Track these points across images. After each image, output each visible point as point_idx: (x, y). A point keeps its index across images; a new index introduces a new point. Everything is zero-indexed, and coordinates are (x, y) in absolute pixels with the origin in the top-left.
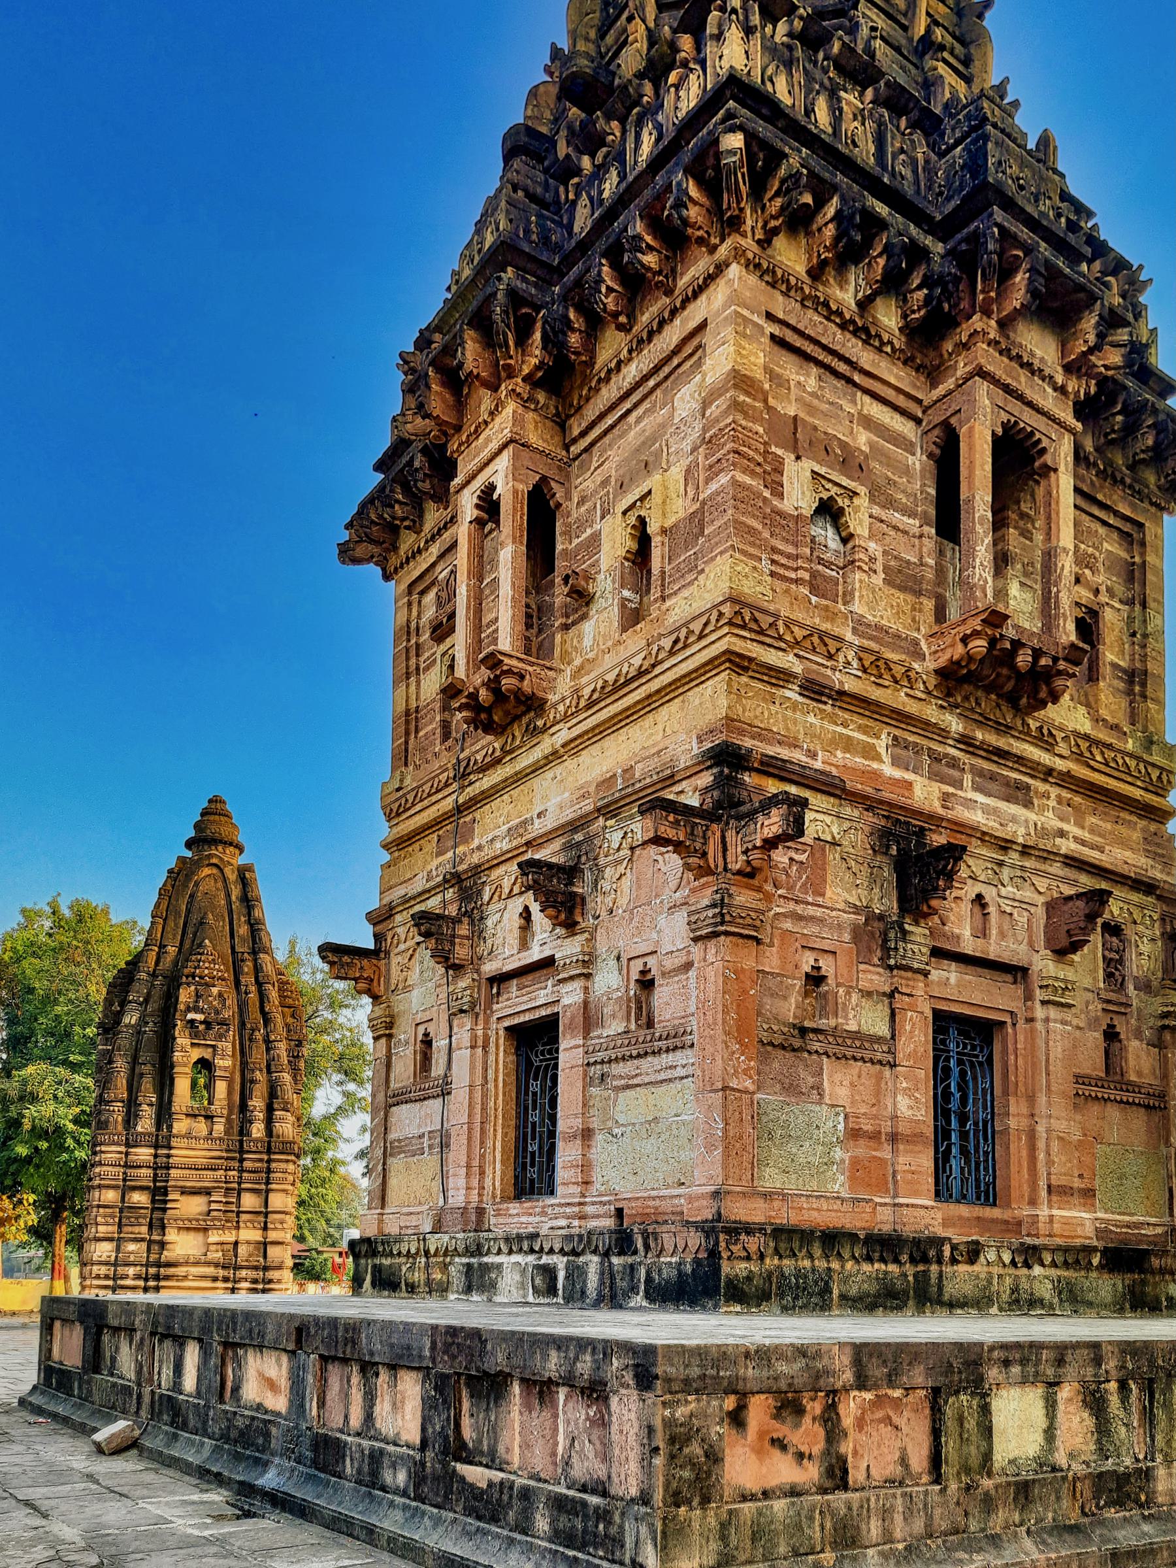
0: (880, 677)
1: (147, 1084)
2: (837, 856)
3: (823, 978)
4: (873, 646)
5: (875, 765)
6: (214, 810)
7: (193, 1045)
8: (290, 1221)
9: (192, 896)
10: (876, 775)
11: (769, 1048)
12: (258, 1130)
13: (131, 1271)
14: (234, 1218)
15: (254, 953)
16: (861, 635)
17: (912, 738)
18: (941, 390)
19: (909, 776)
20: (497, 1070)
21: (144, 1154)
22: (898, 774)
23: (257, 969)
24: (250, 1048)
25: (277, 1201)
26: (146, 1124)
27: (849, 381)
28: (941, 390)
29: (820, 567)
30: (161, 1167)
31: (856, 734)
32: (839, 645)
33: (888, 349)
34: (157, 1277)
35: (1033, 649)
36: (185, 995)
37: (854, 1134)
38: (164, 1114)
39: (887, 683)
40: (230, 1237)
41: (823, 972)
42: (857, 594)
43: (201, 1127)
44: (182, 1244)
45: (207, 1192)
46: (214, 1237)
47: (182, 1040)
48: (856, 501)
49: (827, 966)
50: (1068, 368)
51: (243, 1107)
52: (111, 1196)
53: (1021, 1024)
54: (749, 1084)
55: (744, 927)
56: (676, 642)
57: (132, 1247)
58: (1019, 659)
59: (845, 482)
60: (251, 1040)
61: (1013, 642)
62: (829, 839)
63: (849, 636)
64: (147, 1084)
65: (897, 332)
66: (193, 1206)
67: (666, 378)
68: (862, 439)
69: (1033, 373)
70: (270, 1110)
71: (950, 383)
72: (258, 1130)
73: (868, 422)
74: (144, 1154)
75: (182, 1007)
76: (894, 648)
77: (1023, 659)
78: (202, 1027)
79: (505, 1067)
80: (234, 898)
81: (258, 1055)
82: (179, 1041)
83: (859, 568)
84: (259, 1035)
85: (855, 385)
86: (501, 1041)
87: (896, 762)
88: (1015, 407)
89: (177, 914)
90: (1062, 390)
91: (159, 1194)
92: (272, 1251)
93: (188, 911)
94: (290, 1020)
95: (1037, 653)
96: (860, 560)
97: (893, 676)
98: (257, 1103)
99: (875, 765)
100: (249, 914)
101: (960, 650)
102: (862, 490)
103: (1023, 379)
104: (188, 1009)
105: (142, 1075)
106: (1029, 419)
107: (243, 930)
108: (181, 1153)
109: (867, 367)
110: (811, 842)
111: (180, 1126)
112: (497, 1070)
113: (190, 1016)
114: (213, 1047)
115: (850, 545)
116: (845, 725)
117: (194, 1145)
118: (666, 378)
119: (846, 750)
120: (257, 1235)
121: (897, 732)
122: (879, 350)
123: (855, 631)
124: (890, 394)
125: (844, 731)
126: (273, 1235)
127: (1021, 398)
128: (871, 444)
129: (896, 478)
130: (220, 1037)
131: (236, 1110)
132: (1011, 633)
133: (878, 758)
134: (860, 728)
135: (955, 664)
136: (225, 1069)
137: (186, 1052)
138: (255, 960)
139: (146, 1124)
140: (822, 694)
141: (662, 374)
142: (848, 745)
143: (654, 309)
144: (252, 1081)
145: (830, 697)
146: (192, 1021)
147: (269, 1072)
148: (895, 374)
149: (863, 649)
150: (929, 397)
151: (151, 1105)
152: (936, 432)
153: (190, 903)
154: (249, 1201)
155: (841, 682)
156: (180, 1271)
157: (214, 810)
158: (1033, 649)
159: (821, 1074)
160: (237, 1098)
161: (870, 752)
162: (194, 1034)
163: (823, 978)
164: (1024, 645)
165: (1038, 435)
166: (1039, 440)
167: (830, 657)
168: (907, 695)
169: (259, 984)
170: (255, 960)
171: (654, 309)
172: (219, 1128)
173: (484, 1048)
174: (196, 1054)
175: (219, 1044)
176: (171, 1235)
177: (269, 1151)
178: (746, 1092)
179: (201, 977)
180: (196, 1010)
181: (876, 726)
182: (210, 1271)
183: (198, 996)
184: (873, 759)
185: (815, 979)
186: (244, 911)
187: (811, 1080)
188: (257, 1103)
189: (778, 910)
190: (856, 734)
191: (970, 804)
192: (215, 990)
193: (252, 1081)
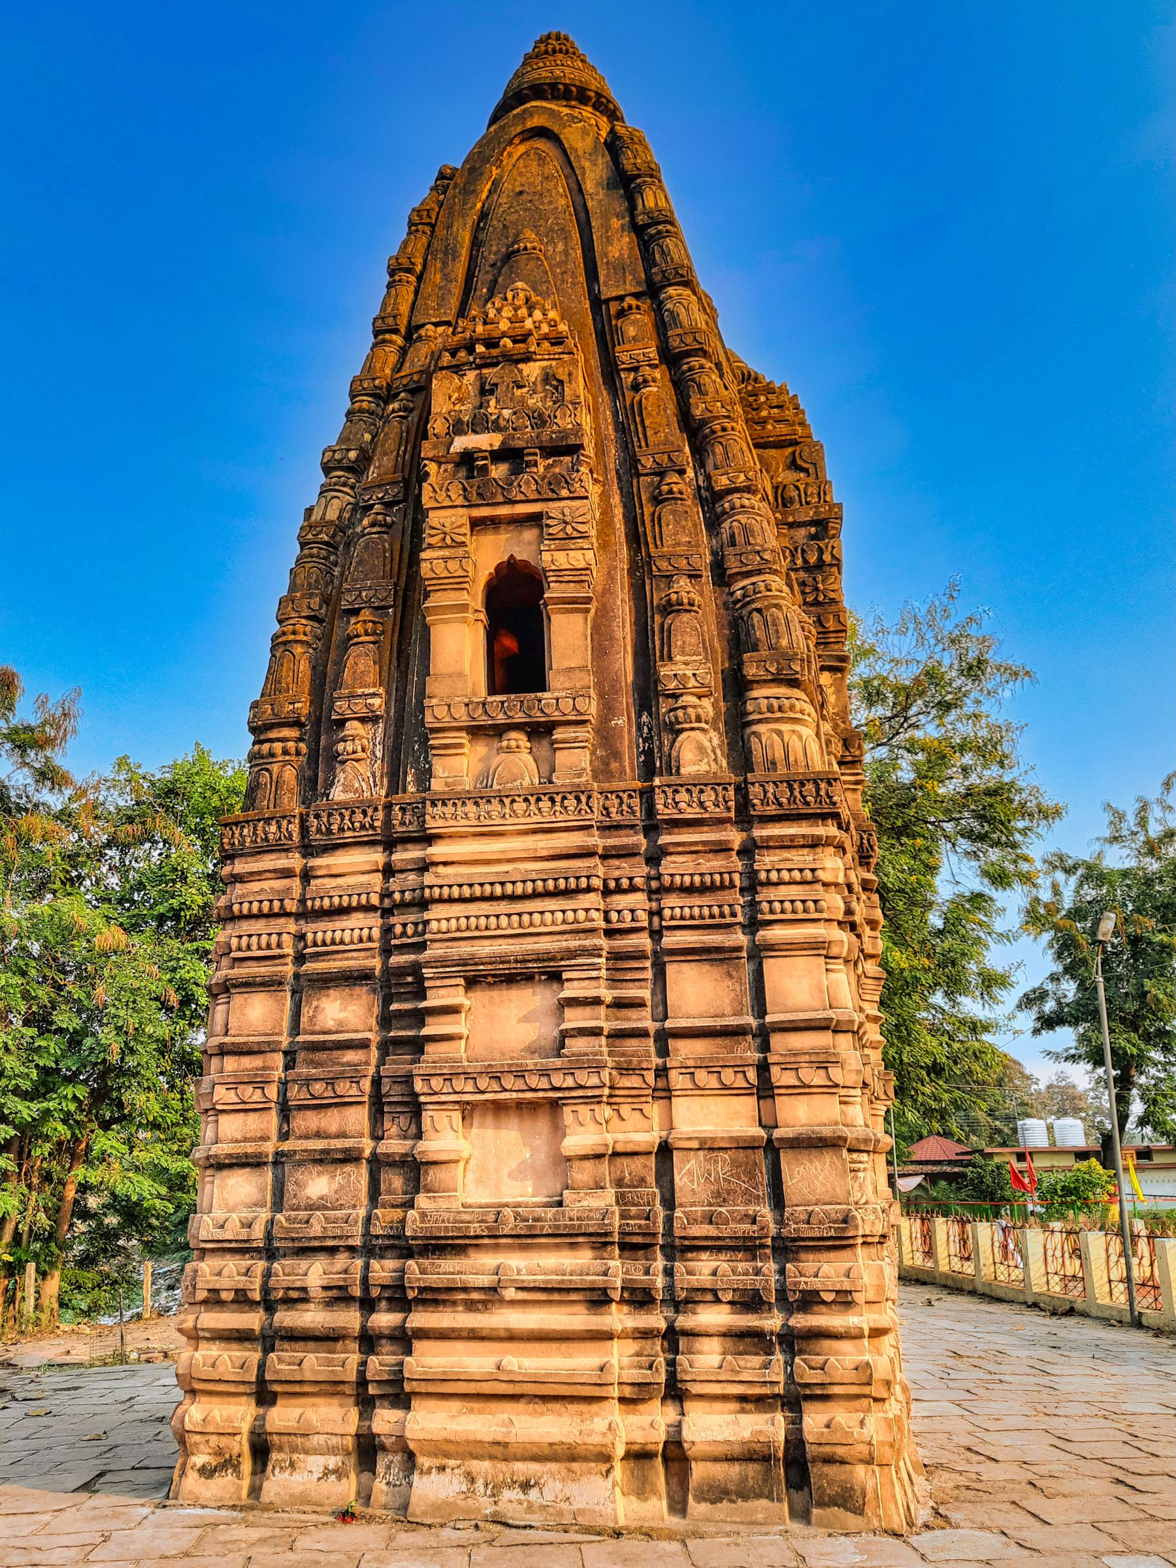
7: (477, 524)
8: (859, 1061)
9: (484, 215)
12: (699, 752)
13: (315, 1274)
14: (651, 1055)
15: (652, 291)
21: (353, 869)
24: (657, 520)
25: (795, 985)
30: (403, 905)
34: (399, 1296)
38: (410, 742)
40: (639, 1130)
43: (520, 762)
44: (482, 1167)
46: (583, 1133)
47: (446, 515)
51: (648, 690)
57: (318, 1185)
60: (657, 500)
66: (500, 1027)
70: (736, 686)
72: (699, 752)
74: (353, 869)
75: (438, 426)
78: (498, 471)
80: (589, 186)
81: (682, 535)
82: (434, 518)
84: (685, 483)
89: (450, 252)
91: (401, 992)
92: (806, 1178)
93: (476, 244)
94: (787, 477)
98: (691, 666)
100: (632, 208)
104: (458, 428)
105: (348, 641)
107: (618, 246)
111: (459, 765)
113: (461, 443)
114: (535, 519)
120: (734, 1118)
126: (799, 1115)
130: (553, 488)
131: (626, 700)
136: (580, 575)
137: (465, 559)
138: (658, 309)
139: (358, 778)
144: (669, 608)
146: (467, 458)
147: (721, 576)
151: (369, 719)
153: (477, 230)
154: (697, 993)
156: (477, 1269)
160: (624, 663)
170: (658, 309)
172: (575, 761)
174: (488, 554)
175: (553, 508)
176: (445, 1137)
177: (745, 817)
179: (491, 343)
180: (479, 424)
182: (575, 1263)
183: (486, 390)
186: (621, 206)
188: (691, 666)
192: (532, 371)
193: (669, 608)
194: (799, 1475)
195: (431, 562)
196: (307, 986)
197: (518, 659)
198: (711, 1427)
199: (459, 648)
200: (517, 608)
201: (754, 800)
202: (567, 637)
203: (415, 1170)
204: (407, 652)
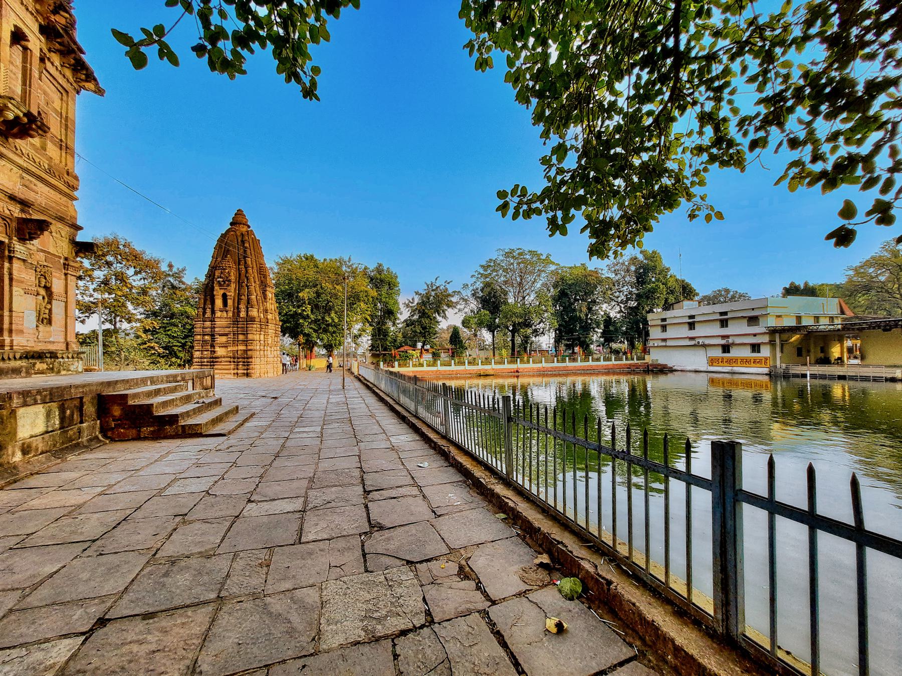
1: (208, 302)
6: (239, 213)
14: (236, 342)
15: (245, 257)
21: (208, 324)
23: (245, 263)
26: (208, 314)
30: (213, 328)
36: (217, 273)
38: (213, 312)
40: (235, 348)
43: (225, 314)
44: (220, 351)
45: (226, 335)
47: (217, 288)
51: (238, 308)
52: (199, 337)
64: (208, 302)
66: (221, 340)
72: (243, 314)
74: (208, 324)
98: (242, 307)
108: (218, 323)
111: (218, 314)
117: (222, 320)
120: (244, 348)
126: (249, 348)
130: (228, 285)
137: (218, 292)
139: (208, 314)
154: (241, 337)
156: (220, 360)
157: (239, 213)
162: (220, 285)
169: (246, 268)
172: (230, 314)
174: (222, 292)
176: (217, 349)
194: (247, 375)
195: (215, 293)
196: (204, 335)
197: (225, 303)
198: (239, 372)
199: (219, 302)
200: (225, 297)
201: (250, 319)
202: (230, 302)
203: (214, 352)
204: (213, 303)
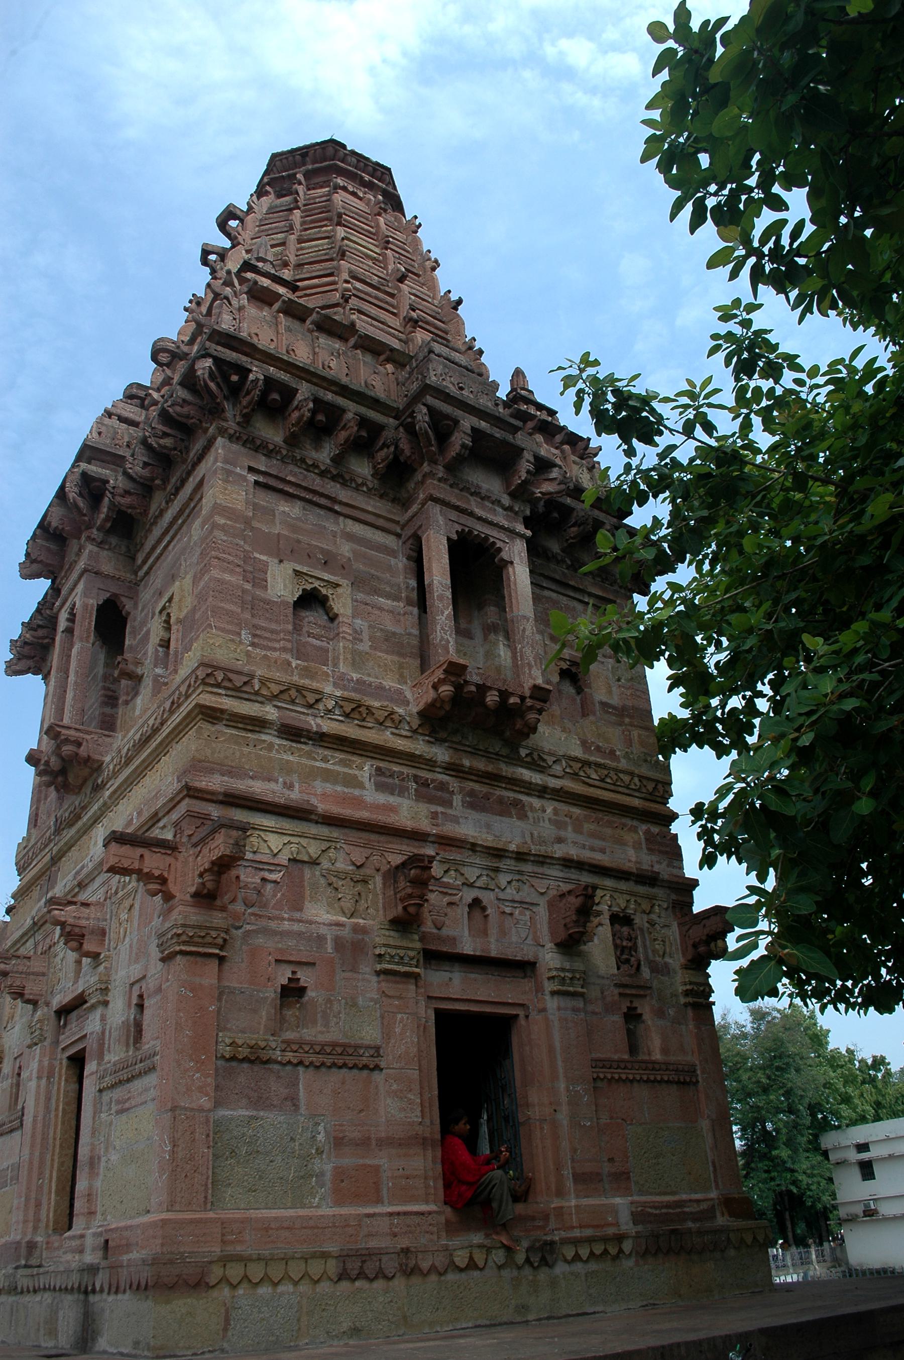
0: (364, 720)
2: (317, 873)
3: (302, 990)
4: (353, 695)
5: (357, 792)
10: (358, 802)
11: (234, 1064)
16: (344, 688)
17: (396, 768)
18: (410, 512)
19: (393, 800)
20: (58, 1099)
22: (382, 798)
27: (331, 510)
28: (410, 512)
29: (310, 639)
31: (337, 768)
32: (318, 697)
33: (365, 489)
35: (499, 691)
37: (338, 1142)
39: (370, 725)
41: (302, 983)
42: (341, 657)
48: (340, 590)
49: (305, 977)
50: (513, 495)
53: (533, 1014)
54: (204, 1102)
55: (204, 945)
56: (173, 703)
58: (488, 699)
59: (326, 576)
61: (478, 686)
62: (306, 859)
63: (328, 689)
65: (370, 478)
67: (188, 516)
68: (346, 549)
69: (482, 499)
71: (415, 508)
73: (350, 537)
76: (377, 697)
77: (492, 698)
79: (65, 1096)
83: (344, 638)
85: (336, 512)
86: (64, 1071)
87: (380, 787)
88: (471, 522)
90: (509, 509)
95: (504, 695)
96: (344, 632)
97: (376, 720)
99: (357, 792)
101: (431, 695)
102: (344, 582)
103: (473, 503)
106: (481, 529)
109: (344, 500)
110: (286, 863)
112: (58, 1099)
115: (336, 622)
116: (325, 760)
118: (188, 516)
119: (325, 780)
121: (382, 764)
122: (357, 489)
123: (335, 685)
124: (370, 518)
125: (324, 765)
127: (471, 514)
128: (354, 552)
129: (378, 574)
132: (476, 679)
133: (361, 786)
134: (342, 762)
135: (431, 706)
140: (301, 736)
141: (186, 514)
142: (328, 776)
143: (178, 474)
145: (310, 739)
148: (373, 505)
149: (345, 699)
150: (403, 519)
152: (410, 541)
155: (318, 725)
158: (499, 691)
159: (295, 1084)
161: (352, 782)
163: (302, 990)
164: (490, 688)
165: (492, 540)
166: (494, 543)
167: (310, 706)
168: (392, 733)
171: (178, 474)
173: (48, 1078)
178: (201, 1110)
181: (357, 760)
184: (355, 787)
185: (292, 992)
187: (284, 1092)
189: (248, 927)
190: (337, 768)
191: (455, 820)
